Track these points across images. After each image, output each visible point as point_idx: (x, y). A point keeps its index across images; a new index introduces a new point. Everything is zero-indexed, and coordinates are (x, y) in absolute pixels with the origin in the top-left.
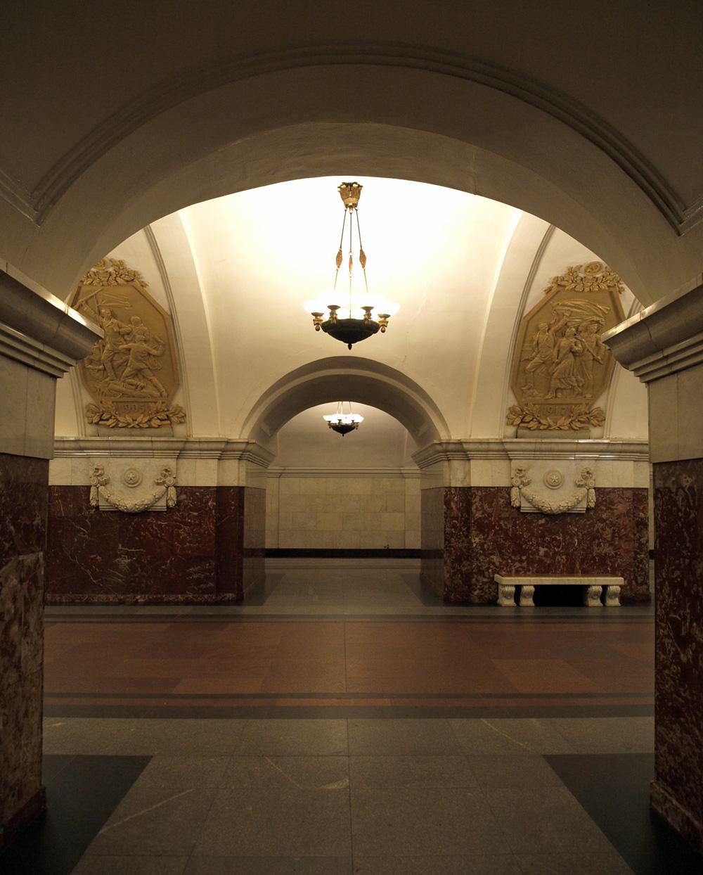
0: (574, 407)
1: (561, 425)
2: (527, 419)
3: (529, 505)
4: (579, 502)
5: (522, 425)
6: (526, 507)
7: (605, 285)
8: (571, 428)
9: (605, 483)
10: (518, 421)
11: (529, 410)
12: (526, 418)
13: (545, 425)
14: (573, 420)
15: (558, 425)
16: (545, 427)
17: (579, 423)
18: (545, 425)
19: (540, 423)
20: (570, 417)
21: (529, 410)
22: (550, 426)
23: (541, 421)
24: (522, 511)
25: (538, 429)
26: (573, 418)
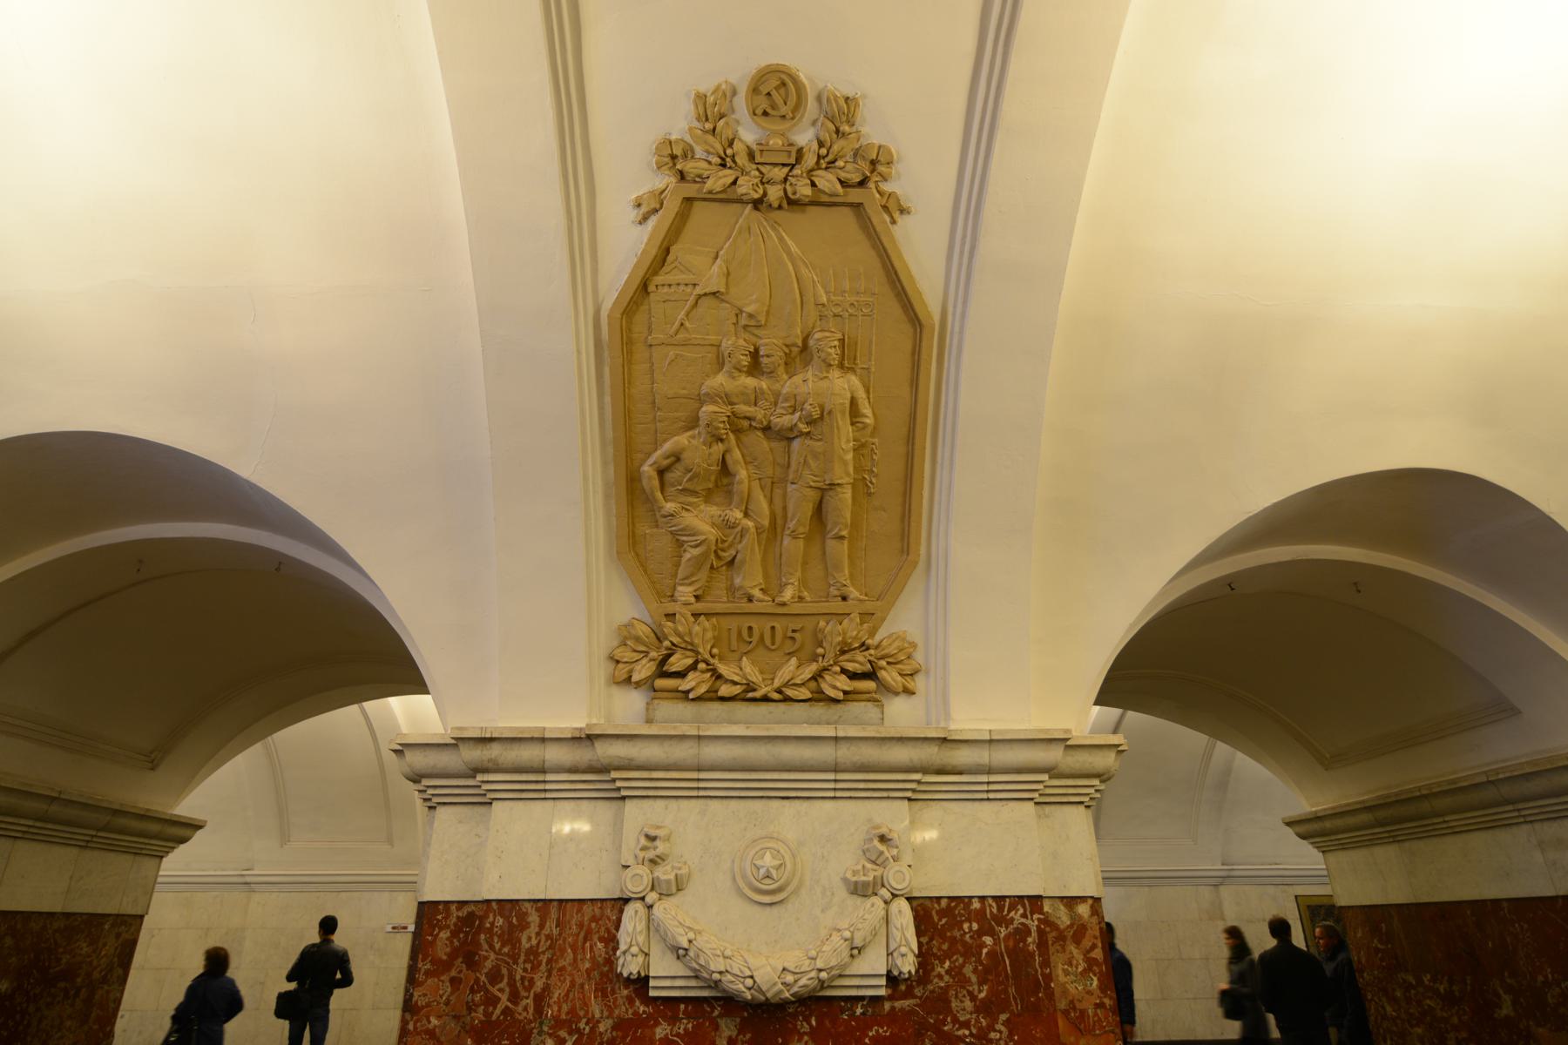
0: (822, 624)
1: (786, 685)
2: (678, 662)
3: (678, 969)
4: (856, 951)
5: (661, 683)
6: (666, 975)
7: (831, 176)
8: (819, 697)
9: (942, 882)
10: (644, 670)
11: (679, 635)
12: (672, 659)
13: (735, 683)
14: (825, 669)
15: (777, 684)
16: (737, 690)
17: (843, 677)
18: (735, 683)
19: (719, 677)
20: (814, 658)
21: (679, 635)
22: (750, 687)
23: (723, 669)
24: (652, 993)
25: (712, 696)
26: (822, 663)
